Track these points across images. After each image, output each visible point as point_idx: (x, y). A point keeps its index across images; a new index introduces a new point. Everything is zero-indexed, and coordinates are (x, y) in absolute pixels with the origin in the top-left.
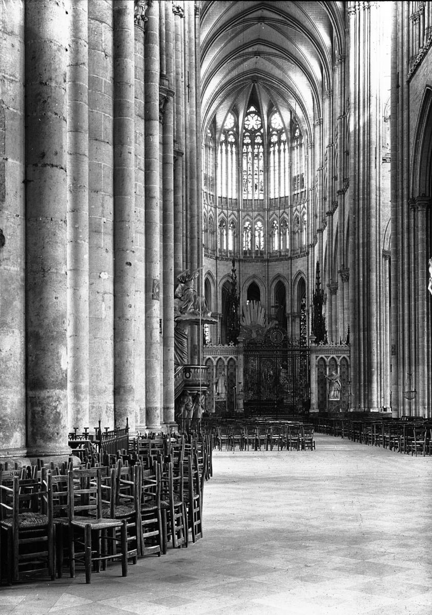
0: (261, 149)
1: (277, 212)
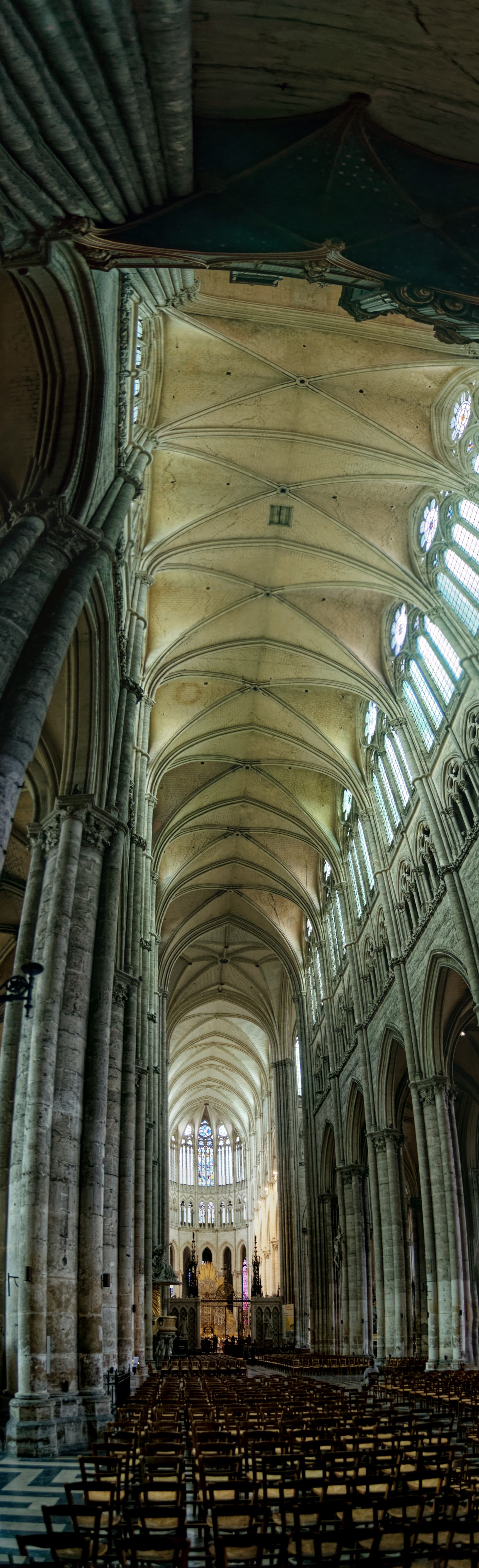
0: (212, 1150)
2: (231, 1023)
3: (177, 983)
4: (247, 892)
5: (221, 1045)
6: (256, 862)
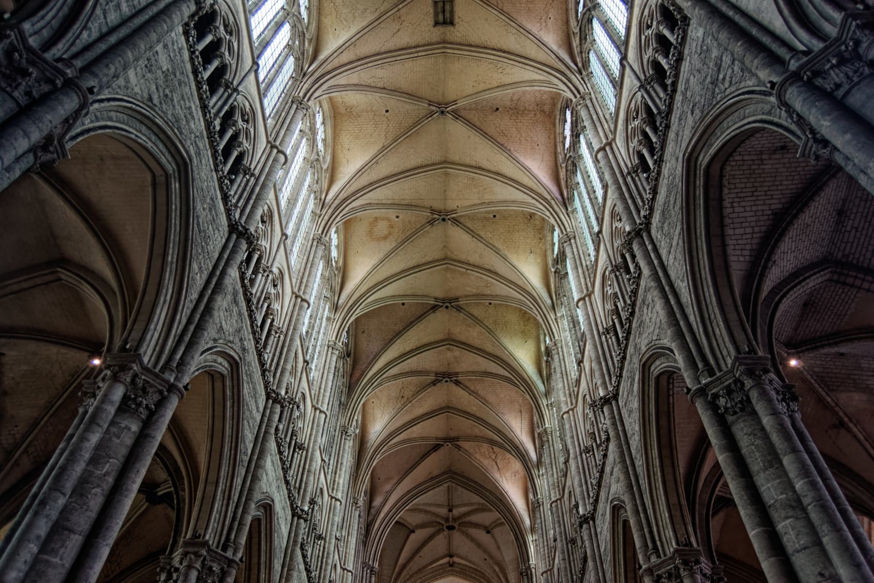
3: (399, 555)
4: (465, 445)
6: (469, 410)
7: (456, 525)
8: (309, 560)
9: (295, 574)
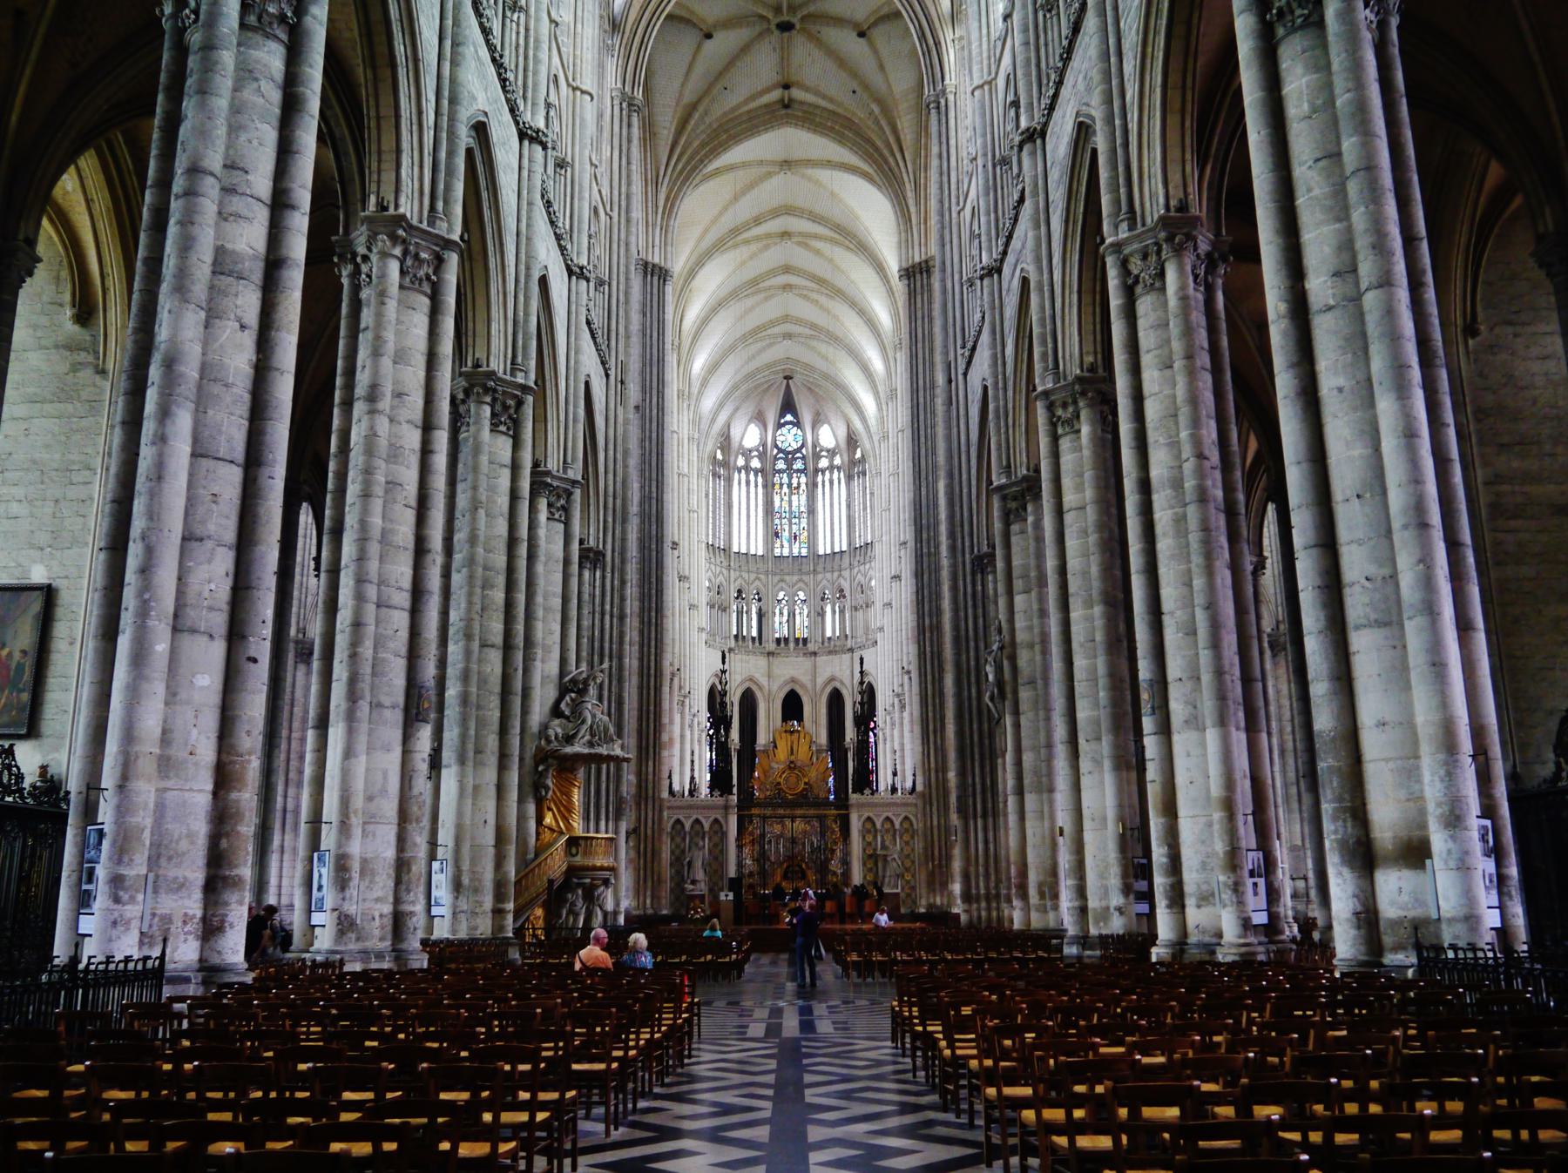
0: (803, 479)
1: (828, 575)
2: (818, 183)
5: (804, 240)
7: (795, 20)
8: (497, 42)
9: (468, 51)
